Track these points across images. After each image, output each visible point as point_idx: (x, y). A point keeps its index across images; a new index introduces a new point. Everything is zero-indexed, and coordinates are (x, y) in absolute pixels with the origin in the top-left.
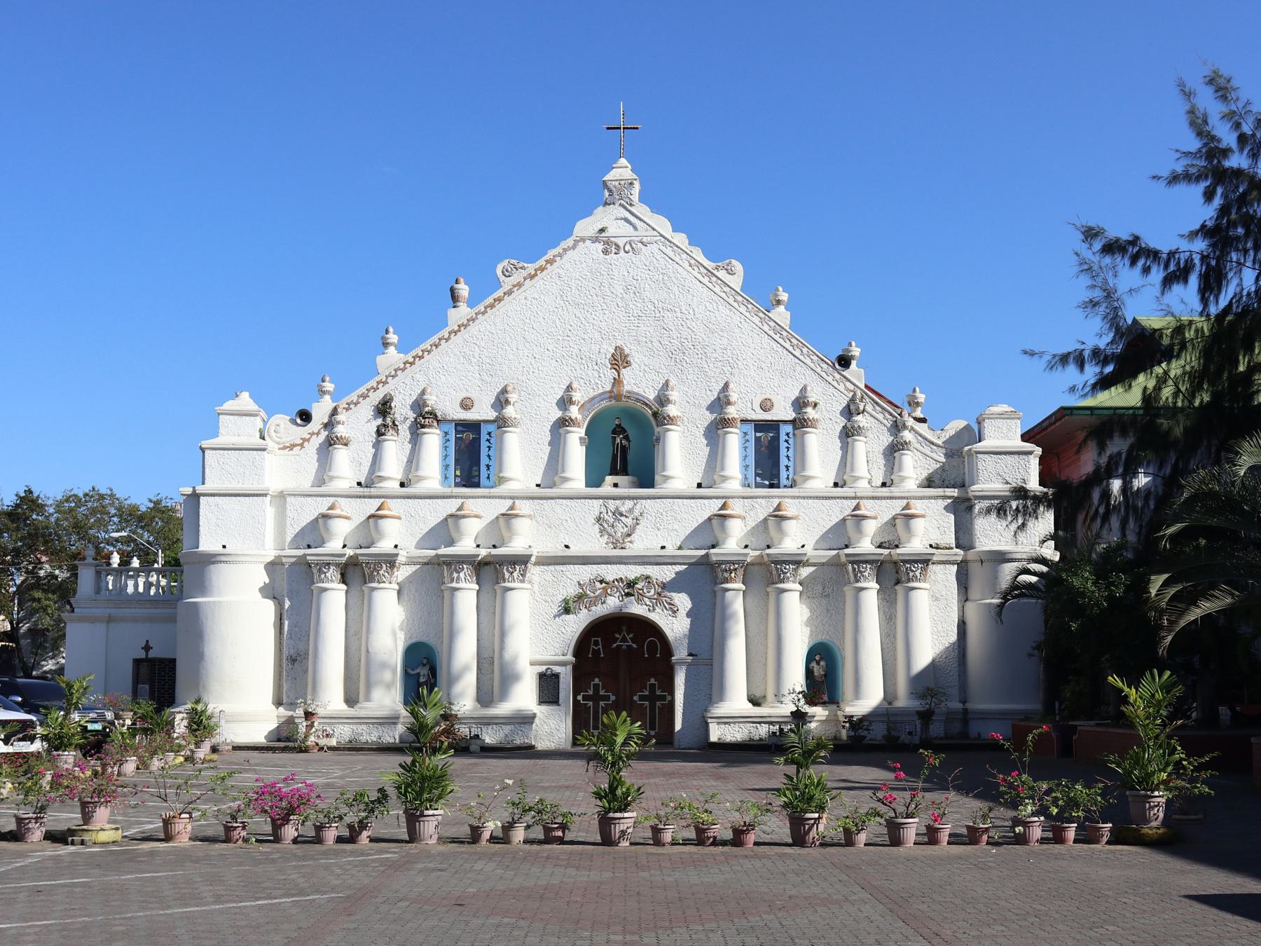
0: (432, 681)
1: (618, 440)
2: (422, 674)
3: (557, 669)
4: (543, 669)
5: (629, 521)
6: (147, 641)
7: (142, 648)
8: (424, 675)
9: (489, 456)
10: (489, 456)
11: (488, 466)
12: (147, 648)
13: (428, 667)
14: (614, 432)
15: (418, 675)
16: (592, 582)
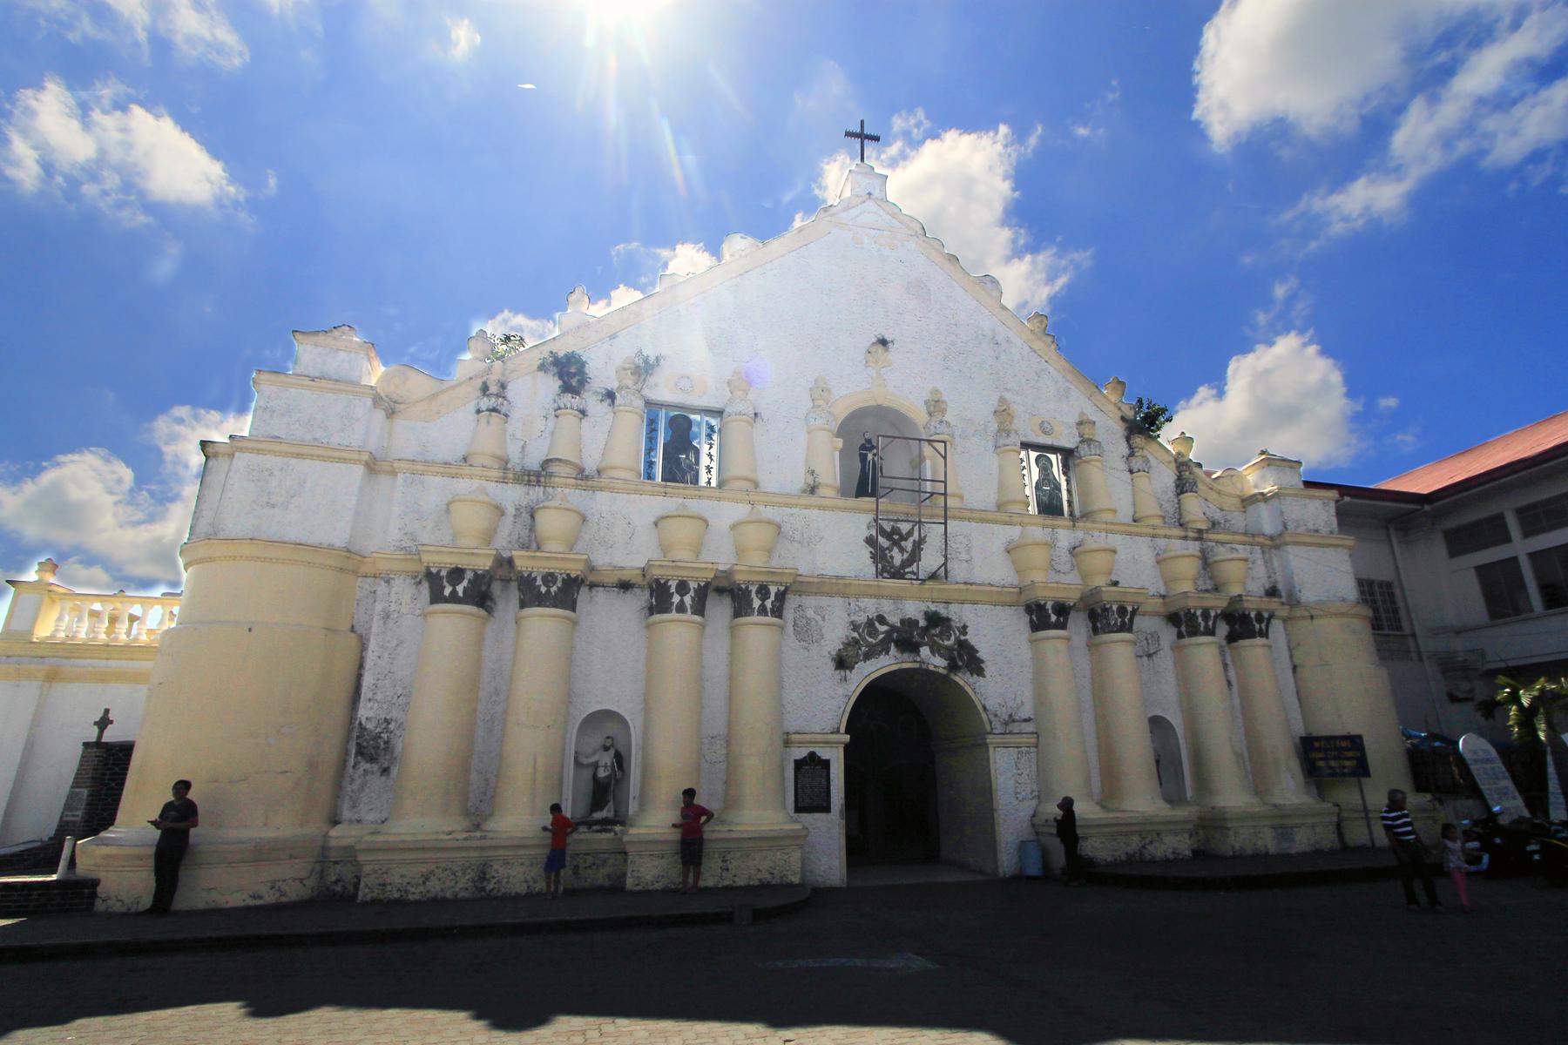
0: (619, 774)
1: (870, 456)
2: (602, 763)
3: (824, 753)
4: (801, 753)
5: (908, 545)
6: (107, 711)
7: (96, 723)
8: (606, 766)
9: (710, 455)
10: (710, 455)
11: (709, 469)
12: (104, 723)
13: (612, 752)
14: (863, 447)
15: (596, 766)
16: (870, 623)
